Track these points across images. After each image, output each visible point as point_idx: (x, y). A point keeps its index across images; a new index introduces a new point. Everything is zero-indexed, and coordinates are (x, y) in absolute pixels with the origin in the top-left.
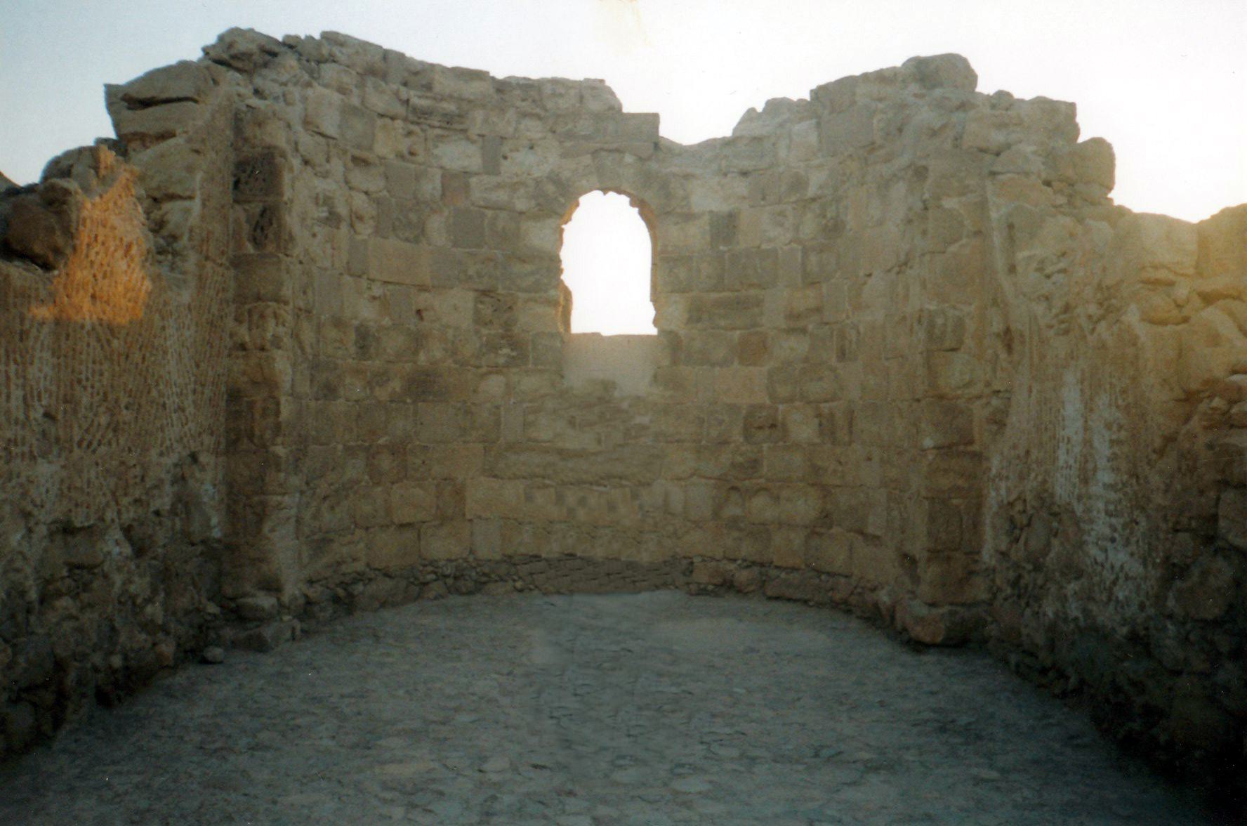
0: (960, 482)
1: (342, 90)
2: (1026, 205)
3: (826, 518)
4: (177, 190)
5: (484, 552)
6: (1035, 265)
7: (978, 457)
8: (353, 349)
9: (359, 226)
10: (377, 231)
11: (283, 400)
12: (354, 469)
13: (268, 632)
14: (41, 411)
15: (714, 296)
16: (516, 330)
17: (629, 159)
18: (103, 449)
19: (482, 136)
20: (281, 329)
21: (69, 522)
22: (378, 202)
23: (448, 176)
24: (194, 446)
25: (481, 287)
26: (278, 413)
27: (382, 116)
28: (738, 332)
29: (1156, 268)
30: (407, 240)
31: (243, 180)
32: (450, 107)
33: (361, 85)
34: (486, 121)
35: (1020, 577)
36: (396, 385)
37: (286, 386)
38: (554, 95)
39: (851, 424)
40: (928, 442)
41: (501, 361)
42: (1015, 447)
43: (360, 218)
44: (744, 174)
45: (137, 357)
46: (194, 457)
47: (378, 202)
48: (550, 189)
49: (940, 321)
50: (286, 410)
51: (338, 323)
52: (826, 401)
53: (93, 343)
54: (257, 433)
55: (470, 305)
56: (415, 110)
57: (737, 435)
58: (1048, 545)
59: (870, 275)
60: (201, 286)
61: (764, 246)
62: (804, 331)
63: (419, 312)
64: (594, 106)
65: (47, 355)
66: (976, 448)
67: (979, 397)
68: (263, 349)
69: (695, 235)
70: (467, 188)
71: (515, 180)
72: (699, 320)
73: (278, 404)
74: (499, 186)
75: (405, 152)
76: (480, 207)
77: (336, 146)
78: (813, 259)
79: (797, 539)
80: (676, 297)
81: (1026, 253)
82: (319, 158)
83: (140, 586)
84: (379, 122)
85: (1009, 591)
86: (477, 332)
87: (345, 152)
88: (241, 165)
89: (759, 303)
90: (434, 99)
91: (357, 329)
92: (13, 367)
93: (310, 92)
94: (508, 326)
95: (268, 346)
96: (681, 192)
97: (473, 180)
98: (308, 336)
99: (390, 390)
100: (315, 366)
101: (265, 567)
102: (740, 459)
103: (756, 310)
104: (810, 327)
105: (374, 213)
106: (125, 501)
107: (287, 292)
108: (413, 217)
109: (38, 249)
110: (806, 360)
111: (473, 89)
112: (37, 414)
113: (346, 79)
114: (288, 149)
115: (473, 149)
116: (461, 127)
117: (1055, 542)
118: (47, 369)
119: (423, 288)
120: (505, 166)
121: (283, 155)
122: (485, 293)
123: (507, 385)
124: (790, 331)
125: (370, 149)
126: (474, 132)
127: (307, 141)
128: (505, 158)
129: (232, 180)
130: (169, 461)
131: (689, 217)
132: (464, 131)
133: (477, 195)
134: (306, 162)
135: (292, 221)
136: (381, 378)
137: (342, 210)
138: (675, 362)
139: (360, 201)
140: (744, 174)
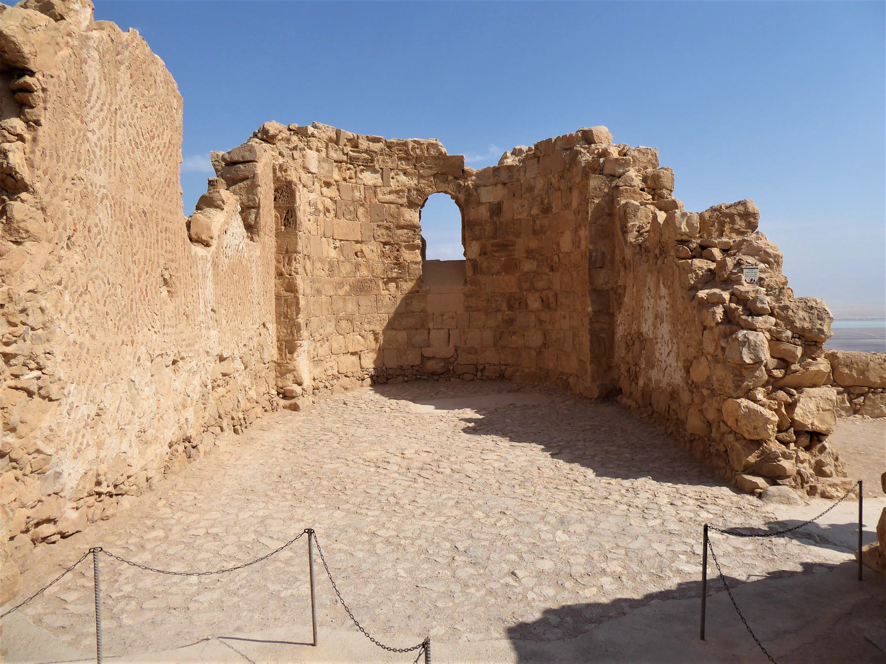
0: (605, 326)
1: (318, 150)
2: (633, 201)
3: (545, 345)
4: (251, 204)
5: (390, 364)
6: (636, 229)
7: (612, 315)
8: (327, 272)
11: (301, 297)
12: (330, 328)
13: (299, 401)
14: (210, 308)
15: (492, 241)
16: (401, 260)
17: (450, 178)
18: (232, 323)
19: (381, 168)
20: (298, 265)
21: (222, 355)
22: (336, 202)
24: (264, 320)
25: (383, 241)
26: (298, 304)
27: (336, 161)
28: (503, 259)
29: (682, 235)
30: (350, 220)
31: (278, 197)
33: (327, 148)
35: (629, 368)
36: (347, 288)
37: (301, 291)
38: (413, 148)
39: (556, 301)
40: (590, 309)
41: (394, 275)
42: (627, 311)
43: (328, 211)
44: (504, 184)
45: (242, 282)
46: (264, 325)
47: (336, 202)
49: (594, 254)
50: (302, 302)
51: (321, 261)
52: (545, 290)
53: (227, 277)
54: (290, 313)
55: (379, 249)
57: (504, 307)
58: (641, 353)
59: (563, 233)
60: (264, 248)
61: (515, 218)
62: (533, 258)
63: (356, 254)
64: (433, 152)
65: (211, 284)
66: (611, 311)
67: (612, 289)
68: (290, 275)
69: (483, 212)
70: (375, 192)
71: (398, 189)
72: (485, 254)
74: (390, 193)
75: (347, 178)
76: (382, 202)
77: (316, 177)
78: (538, 223)
79: (534, 353)
80: (475, 242)
81: (632, 223)
82: (310, 183)
83: (247, 382)
84: (335, 164)
85: (626, 374)
86: (383, 263)
87: (320, 180)
88: (276, 190)
89: (513, 245)
91: (329, 263)
92: (200, 290)
93: (304, 152)
94: (397, 258)
95: (293, 273)
96: (475, 193)
97: (378, 190)
98: (309, 267)
99: (344, 290)
100: (313, 282)
101: (295, 373)
102: (507, 318)
103: (512, 248)
104: (537, 255)
106: (241, 345)
107: (299, 248)
108: (352, 208)
109: (204, 237)
110: (535, 272)
111: (376, 147)
112: (209, 310)
113: (319, 145)
114: (295, 180)
115: (378, 176)
116: (372, 164)
117: (643, 352)
118: (212, 290)
119: (357, 242)
120: (393, 183)
121: (296, 185)
122: (385, 244)
123: (397, 287)
124: (527, 258)
125: (331, 177)
126: (377, 167)
127: (305, 177)
128: (393, 178)
129: (273, 197)
130: (256, 326)
131: (480, 203)
133: (380, 196)
134: (304, 186)
135: (300, 214)
136: (341, 285)
137: (321, 207)
138: (474, 274)
139: (328, 203)
140: (504, 184)
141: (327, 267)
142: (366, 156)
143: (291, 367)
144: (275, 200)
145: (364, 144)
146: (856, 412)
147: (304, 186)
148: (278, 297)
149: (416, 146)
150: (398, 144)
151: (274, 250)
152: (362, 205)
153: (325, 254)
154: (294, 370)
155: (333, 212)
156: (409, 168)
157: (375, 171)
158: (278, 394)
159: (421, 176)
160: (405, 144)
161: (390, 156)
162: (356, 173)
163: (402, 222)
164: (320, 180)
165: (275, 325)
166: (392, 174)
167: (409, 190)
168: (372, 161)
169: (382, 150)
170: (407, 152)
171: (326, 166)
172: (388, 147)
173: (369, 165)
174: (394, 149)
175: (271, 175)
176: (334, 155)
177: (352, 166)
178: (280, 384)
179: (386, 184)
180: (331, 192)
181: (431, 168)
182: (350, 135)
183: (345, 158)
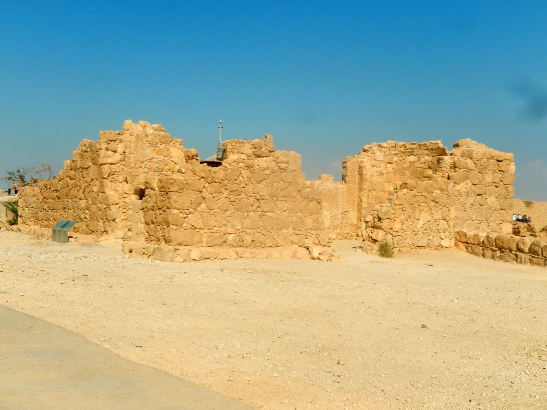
9: (389, 174)
10: (394, 174)
22: (394, 169)
23: (411, 163)
32: (410, 150)
34: (418, 151)
47: (394, 169)
48: (430, 163)
56: (402, 152)
64: (437, 146)
70: (414, 164)
73: (362, 204)
74: (421, 163)
90: (406, 149)
105: (393, 171)
108: (403, 171)
116: (412, 153)
125: (392, 160)
127: (374, 163)
128: (422, 158)
132: (413, 154)
141: (387, 193)
142: (410, 150)
143: (360, 227)
144: (358, 172)
145: (408, 146)
146: (501, 259)
147: (374, 166)
148: (358, 203)
149: (430, 144)
150: (423, 145)
151: (357, 188)
152: (408, 169)
153: (386, 189)
154: (361, 228)
155: (392, 174)
156: (429, 153)
157: (415, 156)
158: (356, 235)
159: (433, 156)
160: (425, 144)
161: (421, 149)
162: (405, 157)
163: (425, 175)
164: (385, 162)
165: (356, 213)
166: (422, 156)
167: (429, 162)
168: (413, 152)
169: (417, 147)
170: (427, 147)
171: (389, 157)
172: (420, 146)
173: (411, 153)
174: (422, 146)
175: (358, 165)
176: (394, 152)
177: (404, 155)
178: (357, 232)
179: (419, 160)
180: (394, 166)
181: (436, 153)
182: (403, 143)
183: (400, 152)
